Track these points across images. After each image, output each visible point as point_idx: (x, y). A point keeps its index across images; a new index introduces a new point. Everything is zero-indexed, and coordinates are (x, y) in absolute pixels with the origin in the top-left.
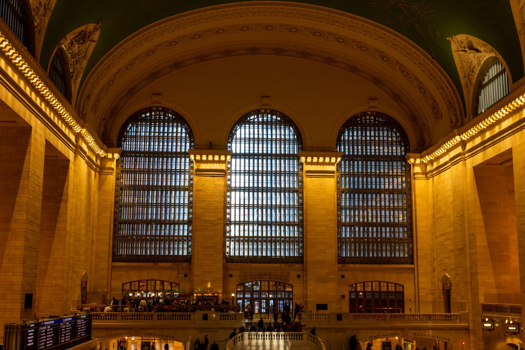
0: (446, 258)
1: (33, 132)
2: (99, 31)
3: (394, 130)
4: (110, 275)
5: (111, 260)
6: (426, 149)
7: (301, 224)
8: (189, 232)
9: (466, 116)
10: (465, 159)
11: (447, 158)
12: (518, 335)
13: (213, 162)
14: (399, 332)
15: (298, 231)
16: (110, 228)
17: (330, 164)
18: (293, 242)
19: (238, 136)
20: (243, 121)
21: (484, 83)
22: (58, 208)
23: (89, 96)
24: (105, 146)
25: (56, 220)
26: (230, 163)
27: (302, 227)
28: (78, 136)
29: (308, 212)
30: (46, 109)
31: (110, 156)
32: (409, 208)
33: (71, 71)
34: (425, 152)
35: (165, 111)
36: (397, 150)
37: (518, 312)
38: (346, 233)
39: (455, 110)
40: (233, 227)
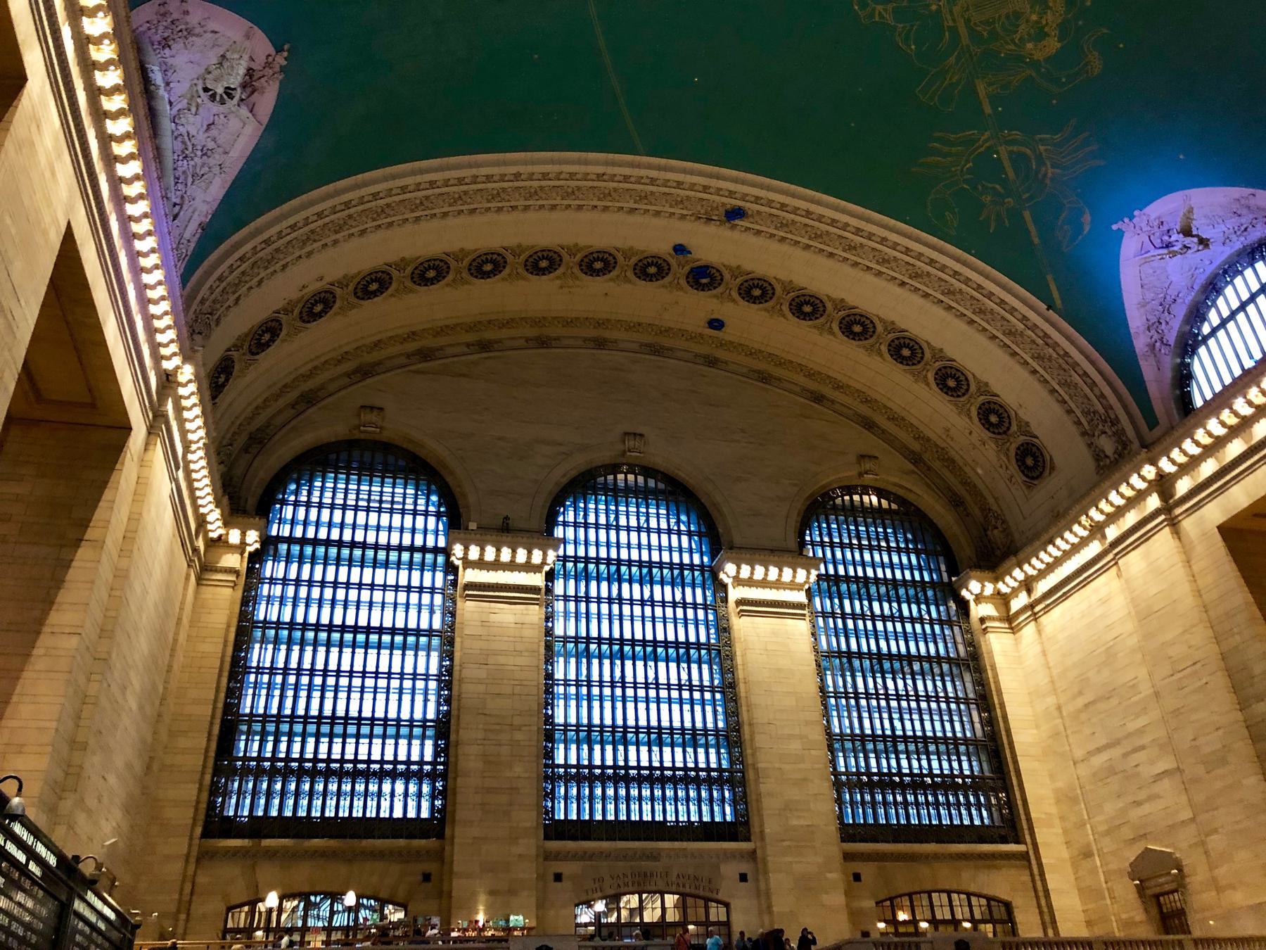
6: (1015, 553)
10: (1174, 524)
11: (1095, 548)
13: (512, 566)
15: (729, 753)
16: (210, 734)
17: (793, 586)
18: (720, 782)
21: (1206, 329)
22: (67, 565)
24: (225, 500)
25: (48, 602)
29: (754, 699)
31: (234, 536)
34: (1013, 560)
39: (1115, 422)
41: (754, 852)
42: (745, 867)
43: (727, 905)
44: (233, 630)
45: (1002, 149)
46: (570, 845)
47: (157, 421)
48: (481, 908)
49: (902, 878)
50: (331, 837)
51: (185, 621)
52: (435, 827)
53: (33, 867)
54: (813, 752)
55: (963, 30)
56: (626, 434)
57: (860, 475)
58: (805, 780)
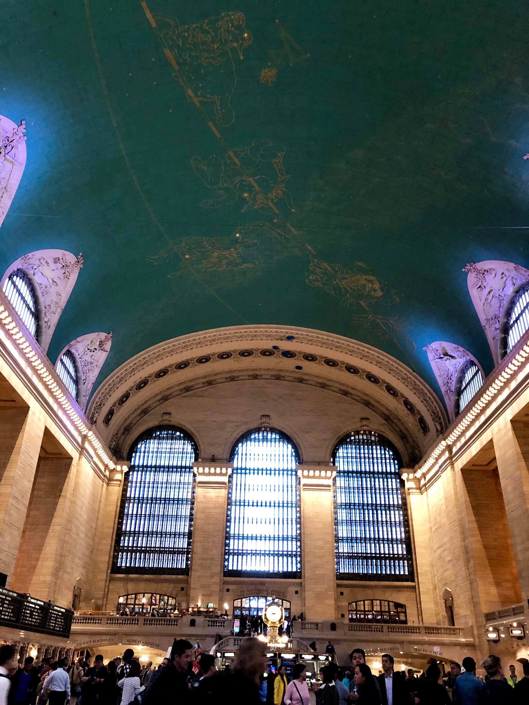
0: (445, 571)
1: (30, 412)
2: (111, 341)
3: (387, 449)
4: (107, 587)
5: (109, 571)
6: (418, 463)
7: (299, 538)
8: (189, 544)
9: (449, 423)
10: (452, 464)
12: (524, 641)
13: (215, 474)
14: (398, 645)
15: (297, 545)
16: (112, 538)
17: (326, 478)
19: (240, 452)
20: (245, 437)
22: (56, 504)
23: (100, 405)
24: (114, 458)
25: (52, 516)
26: (231, 477)
27: (300, 541)
28: (85, 437)
30: (58, 410)
31: (119, 468)
32: (407, 523)
33: (83, 378)
34: (417, 466)
35: (175, 428)
36: (392, 468)
37: (520, 613)
38: (344, 548)
39: (440, 419)
40: (232, 541)
41: (301, 583)
42: (297, 589)
43: (290, 602)
44: (119, 501)
45: (378, 320)
46: (233, 579)
47: (82, 450)
48: (200, 600)
49: (360, 594)
50: (151, 574)
51: (103, 500)
52: (186, 571)
53: (37, 607)
54: (328, 545)
55: (349, 289)
56: (263, 416)
57: (361, 427)
58: (323, 556)
